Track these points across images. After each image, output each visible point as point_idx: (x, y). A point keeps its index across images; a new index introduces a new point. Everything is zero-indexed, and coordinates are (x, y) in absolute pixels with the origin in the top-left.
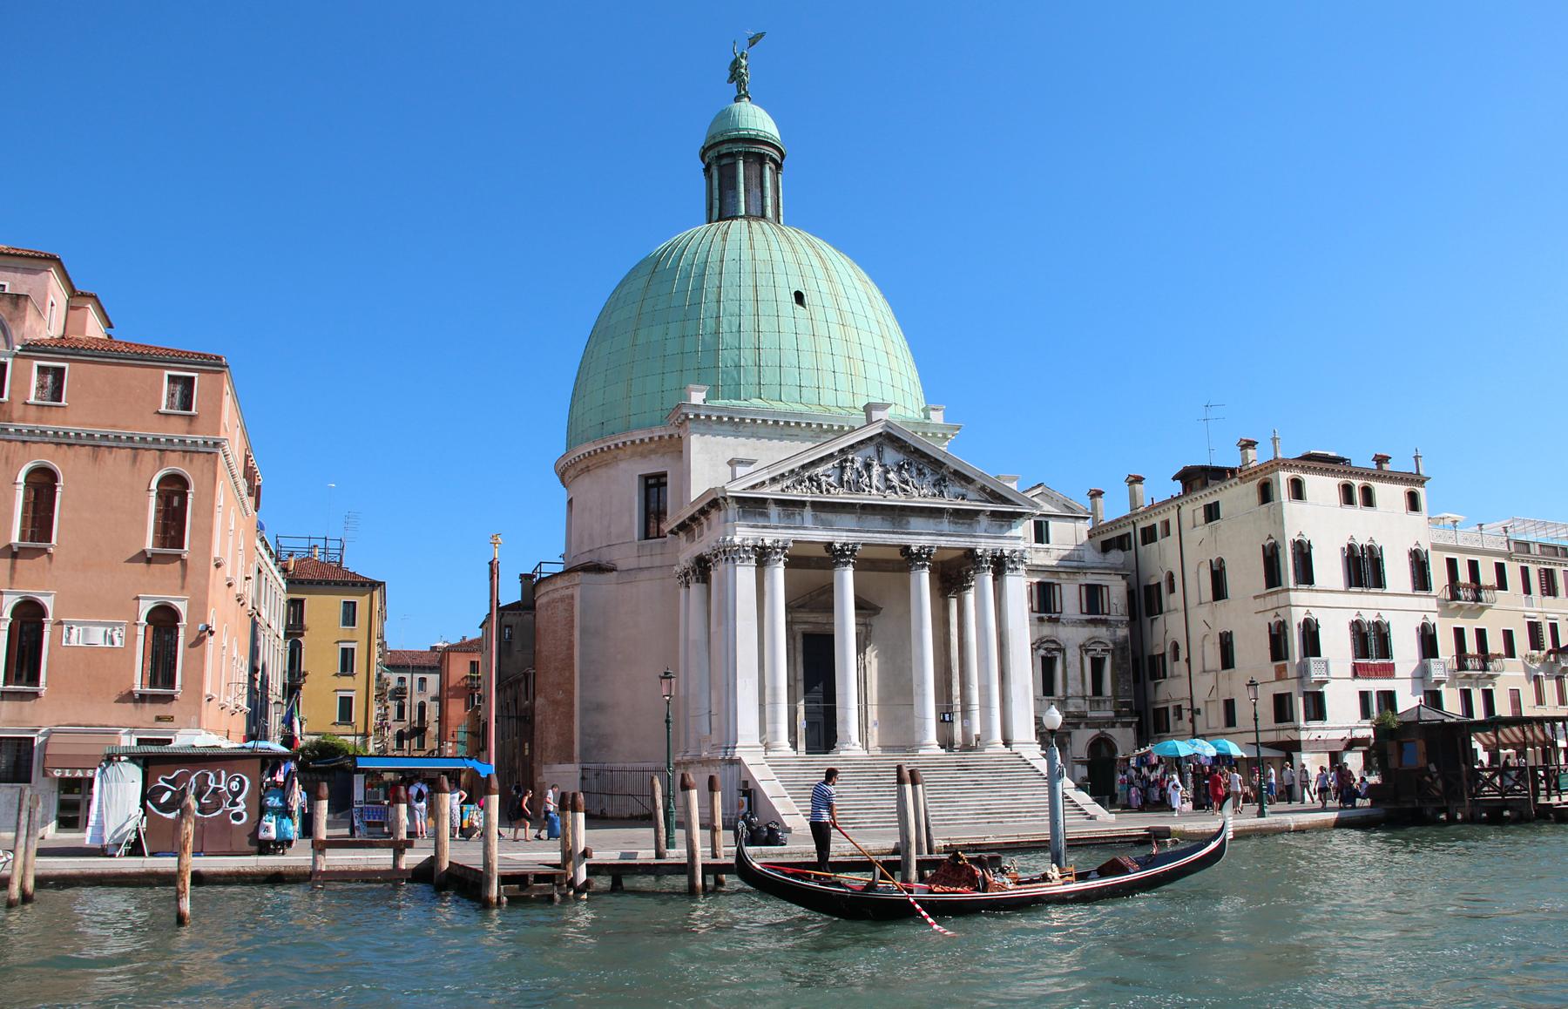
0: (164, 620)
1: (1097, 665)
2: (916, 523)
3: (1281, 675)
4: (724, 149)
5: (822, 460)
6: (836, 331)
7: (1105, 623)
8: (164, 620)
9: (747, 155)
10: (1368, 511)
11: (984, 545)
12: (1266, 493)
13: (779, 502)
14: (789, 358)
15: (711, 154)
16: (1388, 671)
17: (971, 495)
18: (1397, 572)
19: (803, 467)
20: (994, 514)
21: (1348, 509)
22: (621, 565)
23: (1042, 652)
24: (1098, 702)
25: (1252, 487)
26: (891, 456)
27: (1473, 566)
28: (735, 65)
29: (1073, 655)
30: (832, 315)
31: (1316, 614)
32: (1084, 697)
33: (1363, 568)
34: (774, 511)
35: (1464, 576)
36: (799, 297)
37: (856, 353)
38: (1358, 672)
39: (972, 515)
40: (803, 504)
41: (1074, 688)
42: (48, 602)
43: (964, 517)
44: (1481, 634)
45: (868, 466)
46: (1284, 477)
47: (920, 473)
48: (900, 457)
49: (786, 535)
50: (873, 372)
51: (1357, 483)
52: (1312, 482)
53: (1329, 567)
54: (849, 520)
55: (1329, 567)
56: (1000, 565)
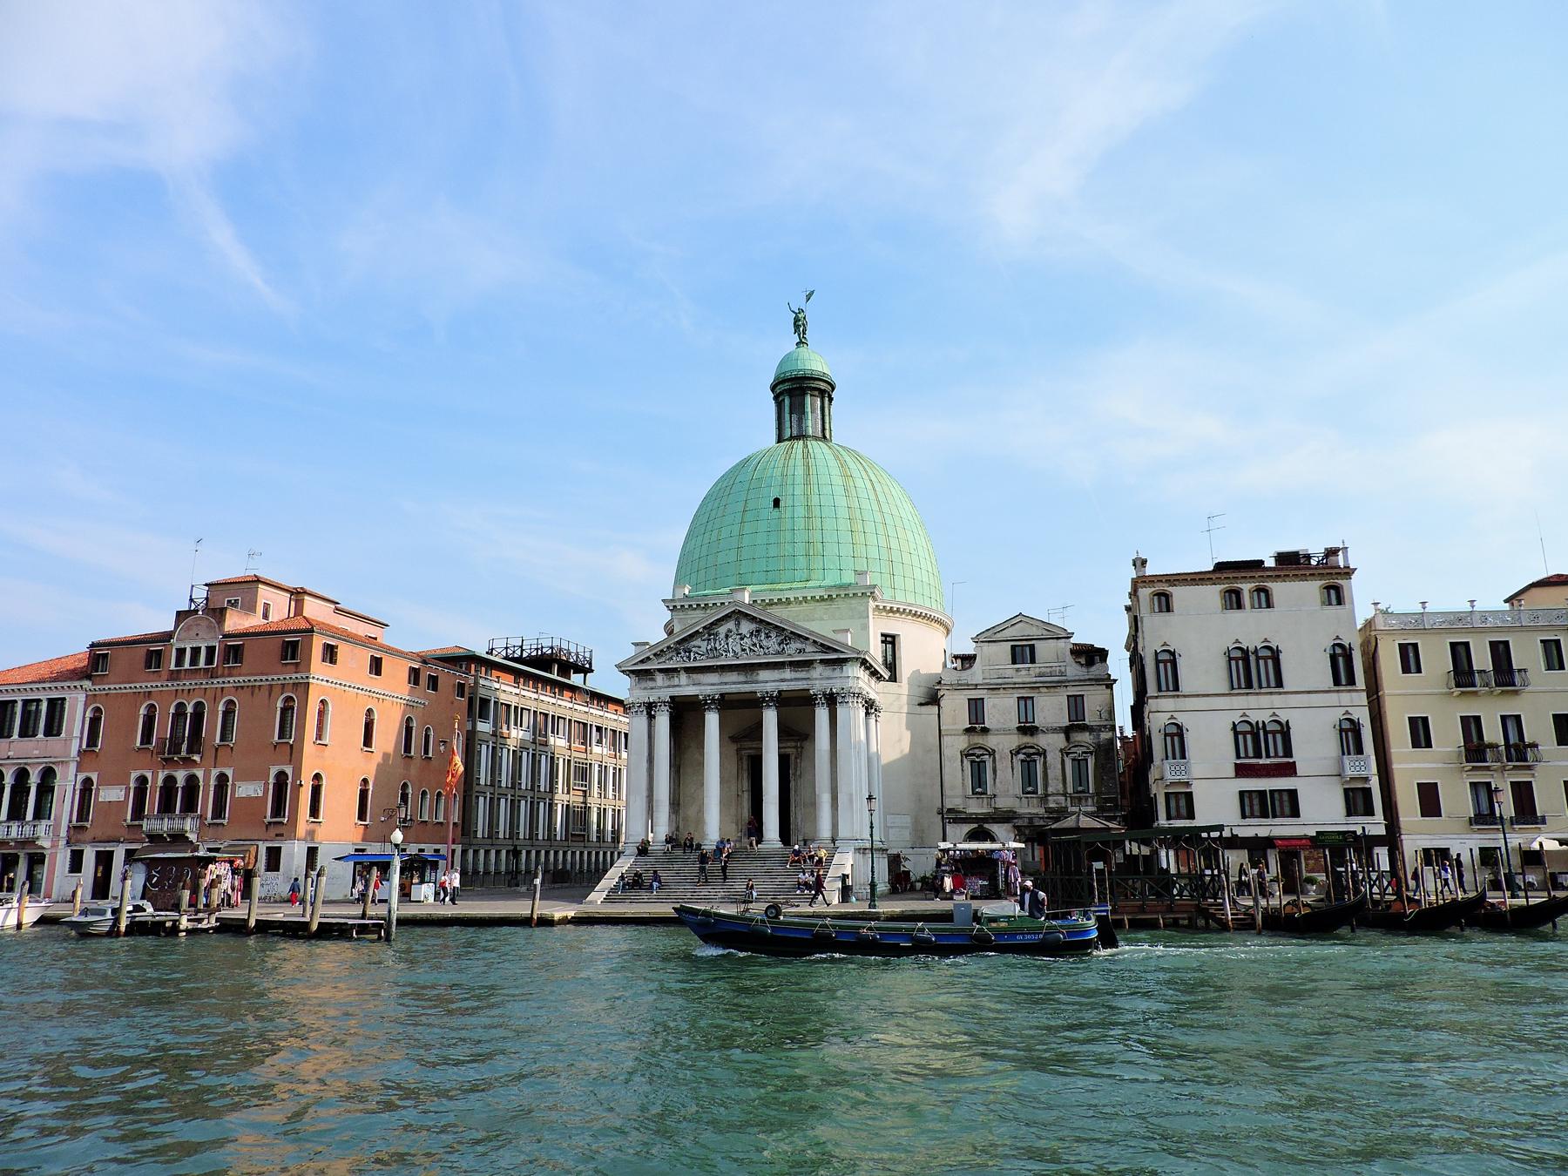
0: (281, 776)
1: (1079, 764)
2: (764, 675)
5: (691, 636)
6: (800, 523)
7: (1085, 728)
8: (281, 776)
9: (790, 392)
13: (660, 670)
16: (1289, 770)
17: (809, 649)
18: (1306, 666)
19: (678, 643)
20: (822, 661)
23: (1021, 756)
24: (1080, 799)
26: (746, 627)
27: (1501, 652)
28: (796, 320)
29: (1054, 758)
30: (800, 511)
31: (1181, 719)
32: (1065, 794)
33: (1254, 668)
34: (659, 678)
35: (1482, 659)
36: (777, 503)
37: (817, 536)
38: (1242, 771)
39: (807, 664)
40: (675, 670)
41: (1055, 786)
42: (229, 772)
44: (1512, 722)
45: (727, 637)
47: (768, 636)
48: (753, 626)
49: (665, 695)
50: (831, 549)
51: (1246, 588)
52: (1178, 593)
53: (1203, 669)
54: (713, 678)
55: (1203, 669)
56: (832, 700)
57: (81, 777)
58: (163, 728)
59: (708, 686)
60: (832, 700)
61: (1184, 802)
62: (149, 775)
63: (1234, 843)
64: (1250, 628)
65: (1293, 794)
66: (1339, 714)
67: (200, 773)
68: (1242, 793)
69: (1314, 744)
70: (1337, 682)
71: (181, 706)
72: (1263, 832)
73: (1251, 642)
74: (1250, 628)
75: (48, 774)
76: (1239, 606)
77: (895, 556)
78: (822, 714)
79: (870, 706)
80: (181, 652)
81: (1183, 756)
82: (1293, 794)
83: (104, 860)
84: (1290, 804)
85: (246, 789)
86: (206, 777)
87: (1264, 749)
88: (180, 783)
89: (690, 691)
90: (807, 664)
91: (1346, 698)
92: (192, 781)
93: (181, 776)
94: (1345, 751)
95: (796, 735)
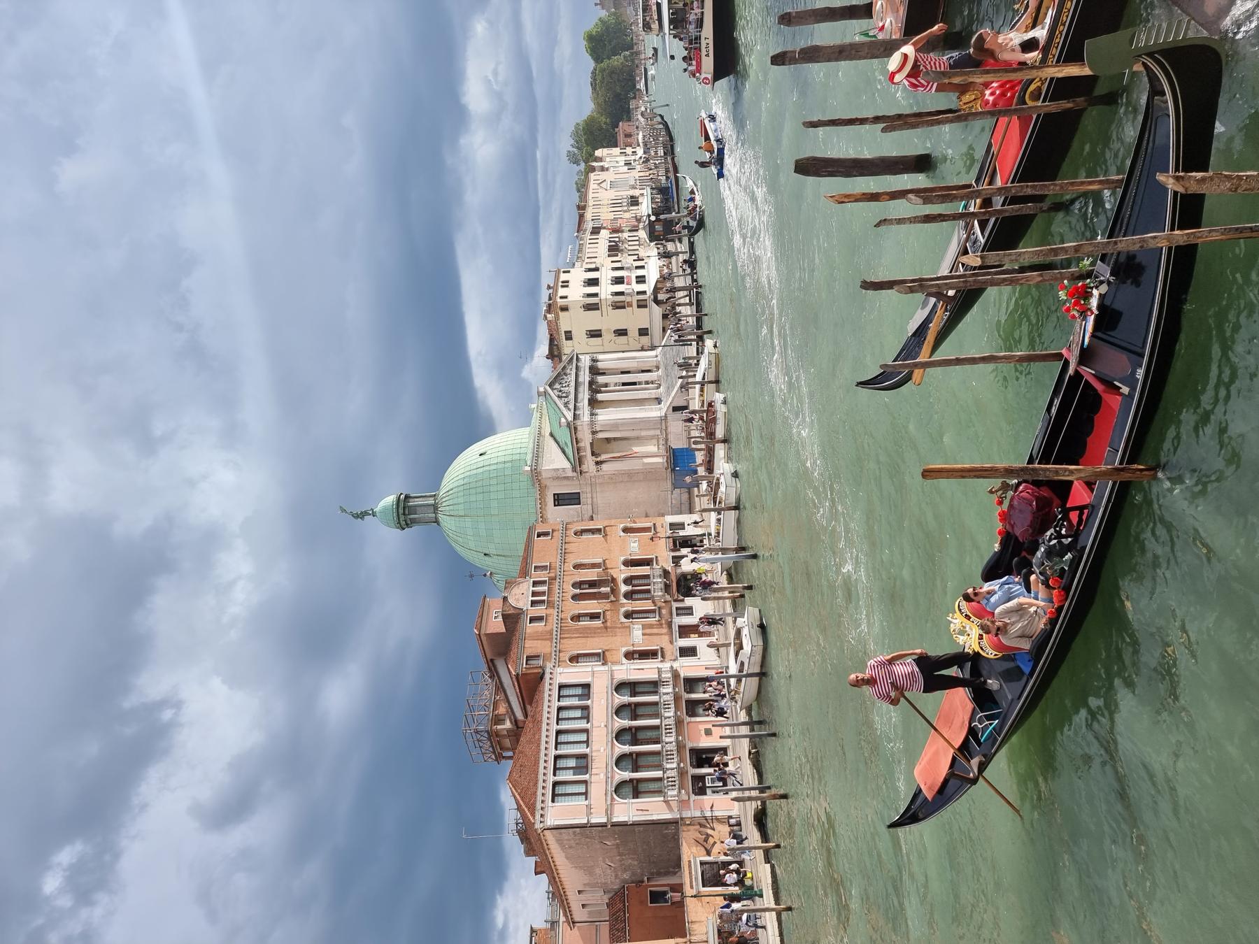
0: (626, 530)
2: (581, 379)
3: (630, 305)
4: (401, 511)
8: (626, 530)
12: (564, 309)
14: (509, 452)
15: (402, 518)
22: (590, 513)
25: (562, 314)
26: (557, 386)
43: (577, 368)
54: (580, 396)
57: (624, 660)
58: (592, 606)
59: (585, 395)
60: (595, 361)
62: (623, 610)
67: (623, 576)
71: (575, 597)
75: (620, 687)
80: (533, 603)
83: (685, 631)
85: (635, 546)
86: (621, 573)
88: (630, 588)
89: (586, 402)
90: (577, 368)
92: (627, 581)
93: (624, 588)
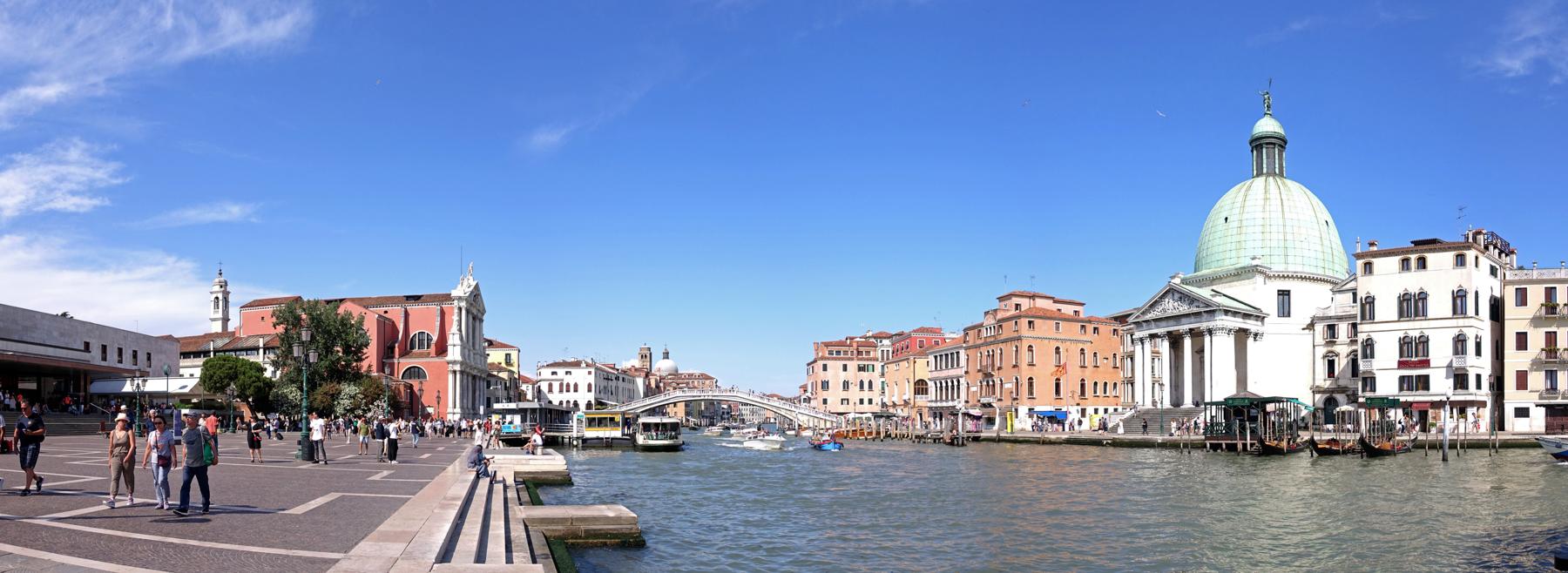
10: (1422, 273)
11: (1204, 325)
16: (1426, 364)
18: (1439, 305)
21: (1406, 275)
30: (1236, 224)
31: (1373, 336)
33: (1413, 305)
37: (1243, 237)
38: (1402, 365)
43: (1198, 314)
46: (1360, 263)
49: (1146, 333)
53: (1386, 308)
55: (1386, 308)
56: (1210, 332)
60: (1210, 332)
61: (1369, 381)
63: (1394, 403)
64: (1413, 282)
65: (1427, 377)
66: (1456, 332)
68: (1402, 379)
69: (1440, 352)
70: (1455, 312)
72: (1410, 399)
73: (1414, 290)
74: (1413, 282)
76: (1408, 269)
77: (1289, 244)
78: (1207, 339)
79: (1242, 335)
81: (1372, 356)
82: (1427, 377)
84: (1424, 383)
87: (1414, 352)
91: (1461, 322)
94: (1456, 352)
95: (1199, 352)
